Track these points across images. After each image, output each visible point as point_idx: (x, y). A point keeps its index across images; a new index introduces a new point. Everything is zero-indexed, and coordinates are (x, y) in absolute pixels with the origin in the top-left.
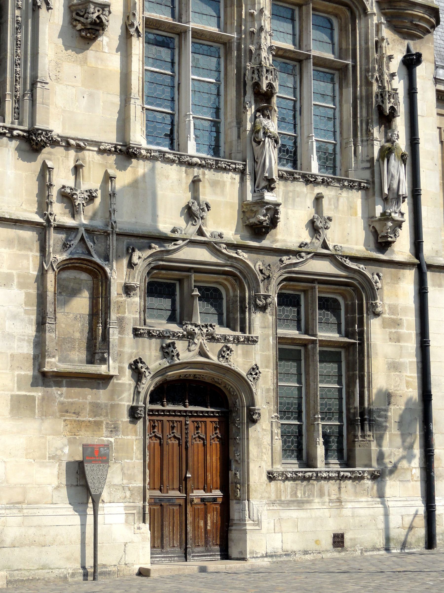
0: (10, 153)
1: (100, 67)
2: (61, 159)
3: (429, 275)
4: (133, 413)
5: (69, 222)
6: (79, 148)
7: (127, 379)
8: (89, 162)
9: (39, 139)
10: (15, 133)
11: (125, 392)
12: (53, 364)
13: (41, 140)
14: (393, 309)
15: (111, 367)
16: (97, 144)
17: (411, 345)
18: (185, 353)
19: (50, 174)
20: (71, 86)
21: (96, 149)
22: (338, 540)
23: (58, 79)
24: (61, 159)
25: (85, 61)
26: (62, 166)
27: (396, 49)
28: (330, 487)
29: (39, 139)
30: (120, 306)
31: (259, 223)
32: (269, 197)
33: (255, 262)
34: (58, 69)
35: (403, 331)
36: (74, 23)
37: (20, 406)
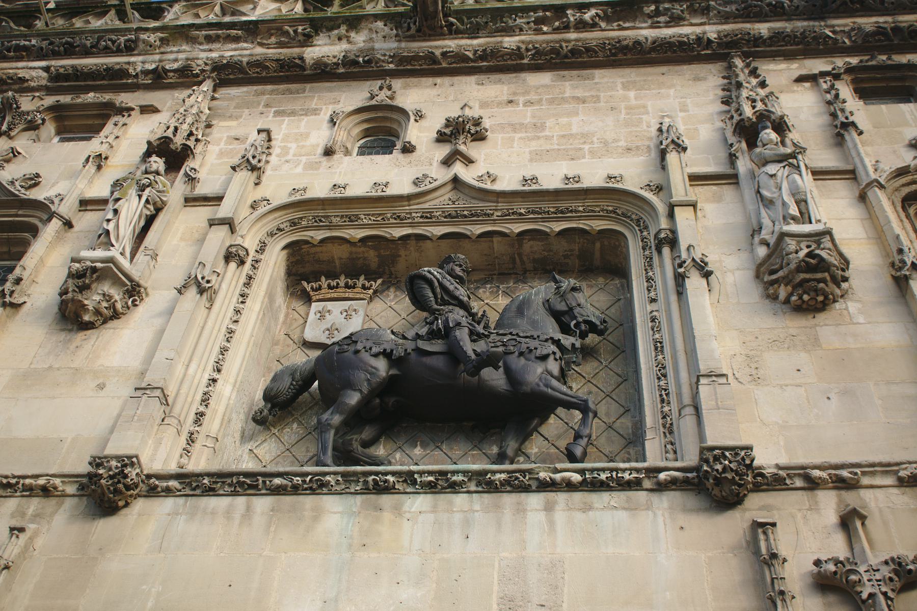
0: (660, 520)
1: (853, 346)
2: (799, 515)
6: (843, 484)
8: (880, 511)
9: (719, 467)
10: (662, 476)
13: (725, 469)
16: (887, 468)
19: (767, 540)
20: (792, 385)
21: (889, 480)
23: (756, 380)
24: (799, 515)
25: (816, 342)
29: (719, 467)
34: (753, 366)
36: (771, 291)
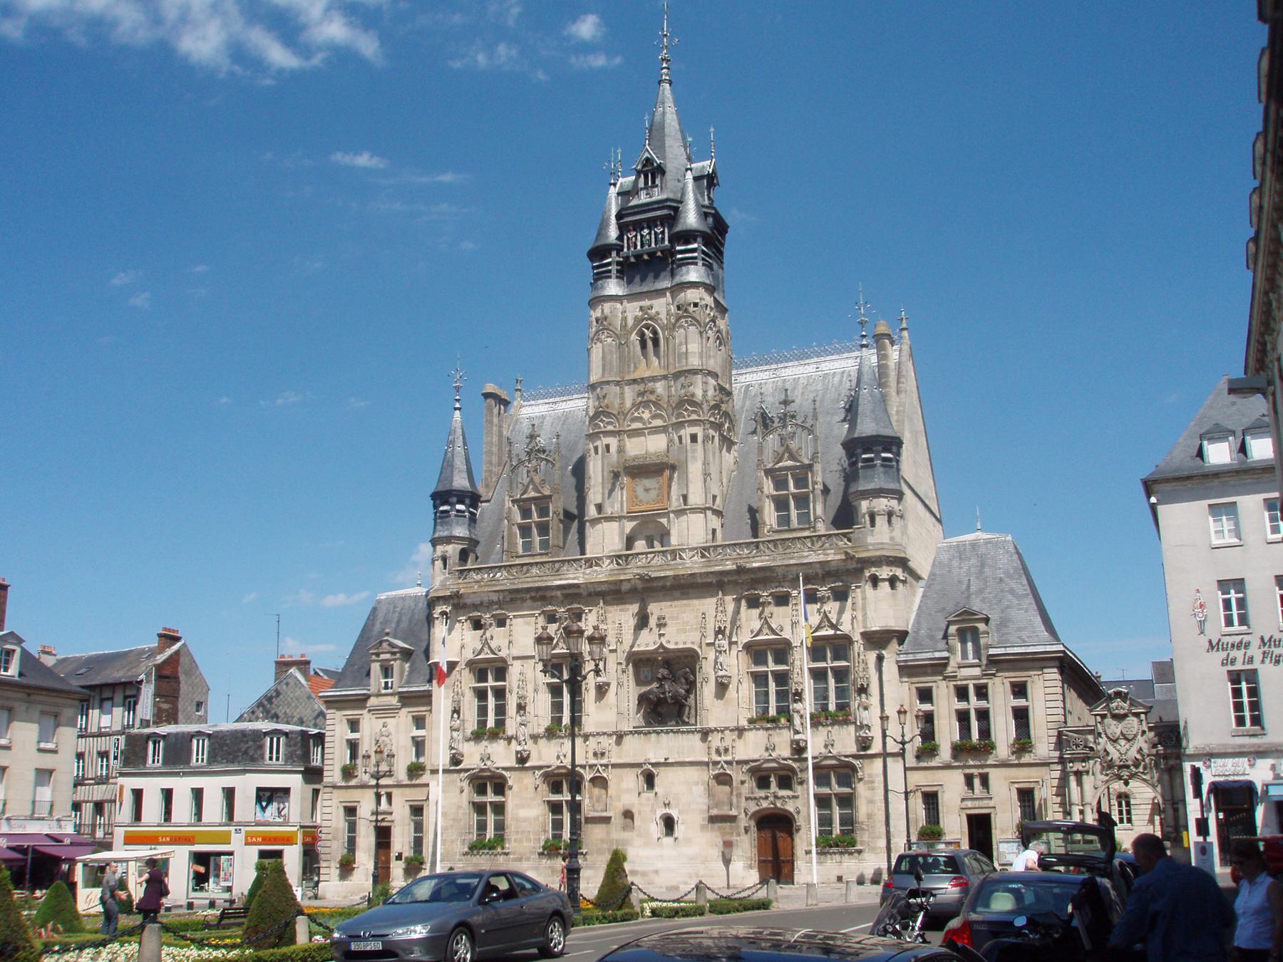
3: (889, 760)
4: (747, 830)
5: (718, 759)
7: (743, 815)
11: (743, 821)
12: (714, 812)
14: (870, 776)
15: (733, 812)
17: (882, 791)
18: (765, 804)
22: (840, 879)
26: (715, 740)
27: (872, 656)
28: (838, 856)
30: (738, 788)
31: (799, 749)
32: (797, 737)
33: (795, 765)
35: (876, 785)
37: (703, 828)
